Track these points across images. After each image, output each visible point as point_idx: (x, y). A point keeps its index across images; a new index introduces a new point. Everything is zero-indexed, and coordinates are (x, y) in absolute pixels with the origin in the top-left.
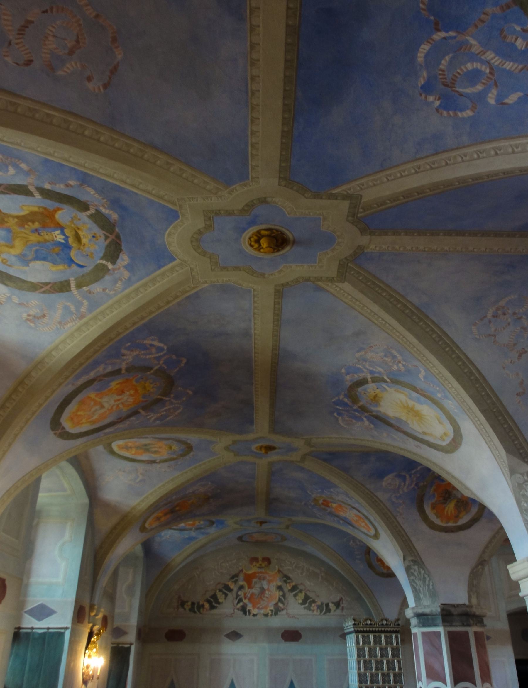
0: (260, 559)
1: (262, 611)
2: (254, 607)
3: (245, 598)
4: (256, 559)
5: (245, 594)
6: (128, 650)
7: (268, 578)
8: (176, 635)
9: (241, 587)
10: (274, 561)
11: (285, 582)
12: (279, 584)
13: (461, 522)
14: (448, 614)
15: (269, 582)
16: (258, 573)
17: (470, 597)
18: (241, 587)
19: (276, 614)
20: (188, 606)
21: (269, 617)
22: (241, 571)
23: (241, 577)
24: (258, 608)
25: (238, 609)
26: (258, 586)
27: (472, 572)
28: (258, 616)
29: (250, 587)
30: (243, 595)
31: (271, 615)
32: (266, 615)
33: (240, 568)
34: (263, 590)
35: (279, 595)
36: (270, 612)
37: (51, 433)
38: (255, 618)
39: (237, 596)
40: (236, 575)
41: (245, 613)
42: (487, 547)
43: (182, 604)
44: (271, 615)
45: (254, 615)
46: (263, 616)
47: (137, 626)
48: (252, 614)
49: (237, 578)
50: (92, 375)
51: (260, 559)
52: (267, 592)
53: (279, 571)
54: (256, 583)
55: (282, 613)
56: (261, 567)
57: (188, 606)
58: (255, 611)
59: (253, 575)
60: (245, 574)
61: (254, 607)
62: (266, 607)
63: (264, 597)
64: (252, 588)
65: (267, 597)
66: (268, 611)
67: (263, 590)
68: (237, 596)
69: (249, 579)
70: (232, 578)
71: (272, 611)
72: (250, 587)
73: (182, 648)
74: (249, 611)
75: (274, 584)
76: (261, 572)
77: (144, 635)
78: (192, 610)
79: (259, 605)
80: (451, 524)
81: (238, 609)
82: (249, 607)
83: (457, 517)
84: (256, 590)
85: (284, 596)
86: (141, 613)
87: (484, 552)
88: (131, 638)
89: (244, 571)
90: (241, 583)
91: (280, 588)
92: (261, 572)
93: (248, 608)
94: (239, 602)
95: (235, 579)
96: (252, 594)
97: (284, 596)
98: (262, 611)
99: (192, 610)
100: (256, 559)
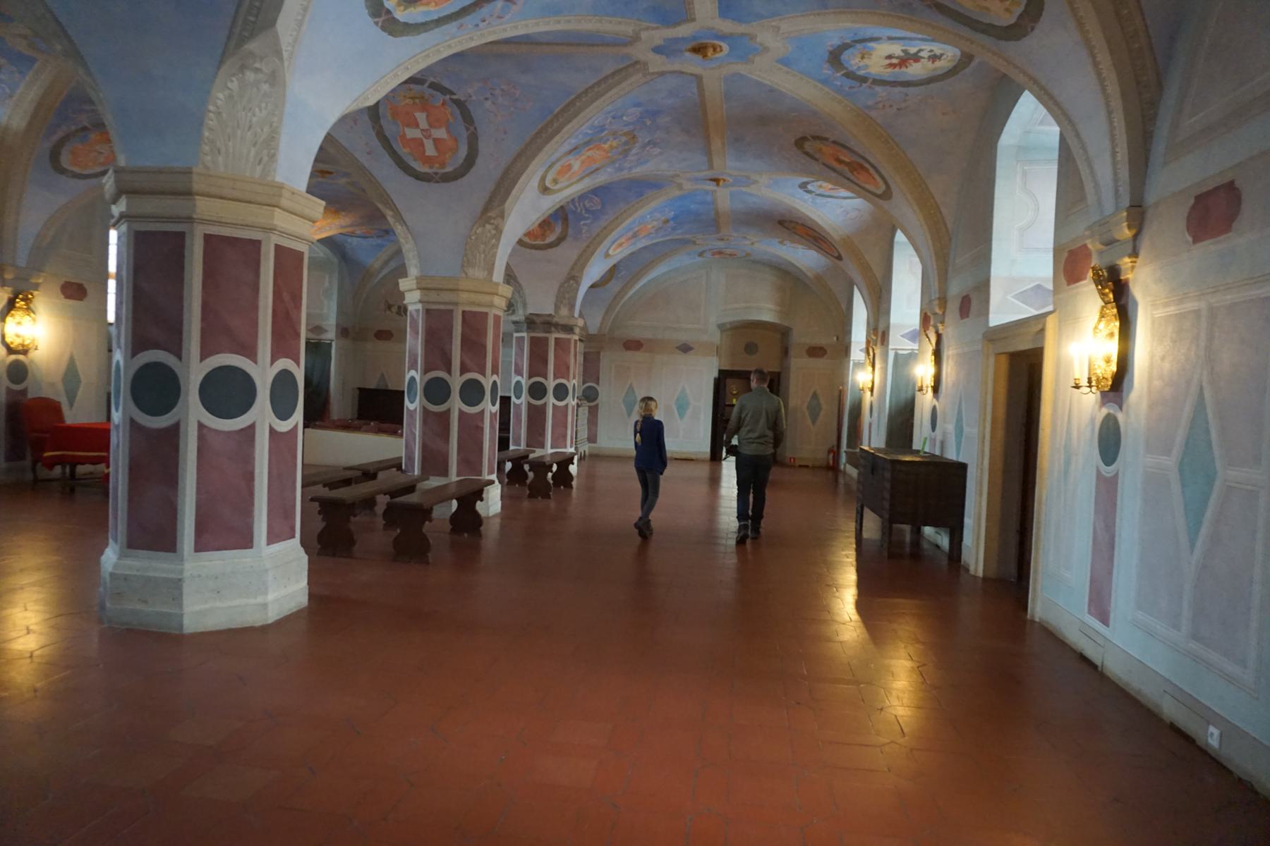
6: (330, 345)
8: (384, 335)
13: (548, 240)
14: (531, 323)
17: (557, 308)
20: (394, 309)
27: (561, 286)
37: (64, 177)
42: (575, 264)
43: (389, 307)
47: (337, 325)
50: (60, 134)
57: (394, 309)
73: (383, 345)
77: (343, 332)
78: (399, 313)
80: (539, 242)
83: (543, 236)
86: (341, 312)
87: (573, 269)
88: (330, 335)
99: (399, 313)
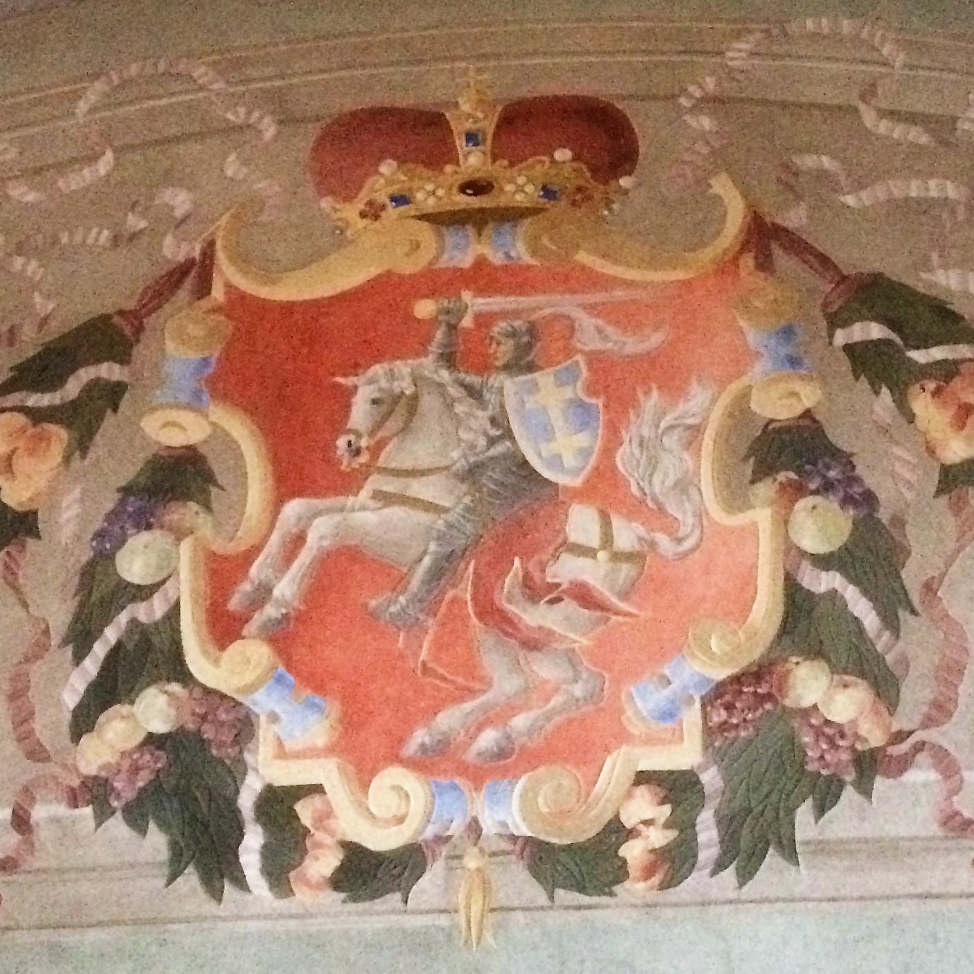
0: (469, 111)
1: (508, 811)
2: (363, 750)
3: (224, 629)
4: (419, 133)
5: (223, 572)
7: (592, 334)
9: (177, 479)
10: (675, 135)
11: (871, 363)
12: (780, 400)
15: (614, 390)
16: (439, 282)
18: (177, 479)
19: (756, 838)
21: (635, 888)
22: (197, 273)
23: (181, 345)
24: (436, 761)
25: (94, 793)
26: (433, 452)
28: (428, 886)
29: (304, 467)
30: (187, 590)
31: (675, 862)
32: (581, 865)
33: (175, 250)
34: (513, 498)
35: (792, 554)
36: (642, 808)
38: (379, 916)
39: (99, 593)
40: (109, 337)
41: (207, 848)
44: (675, 862)
45: (364, 873)
46: (517, 883)
48: (323, 862)
49: (109, 371)
51: (469, 111)
52: (582, 523)
53: (763, 237)
54: (399, 410)
55: (847, 818)
56: (478, 212)
58: (385, 810)
59: (374, 320)
60: (239, 302)
61: (363, 750)
62: (577, 742)
63: (534, 590)
64: (348, 483)
65: (584, 596)
66: (613, 789)
67: (513, 498)
68: (99, 593)
69: (293, 376)
70: (44, 369)
71: (677, 789)
72: (304, 467)
74: (279, 805)
75: (703, 402)
76: (482, 277)
79: (449, 719)
81: (94, 793)
82: (289, 743)
84: (400, 508)
85: (873, 554)
89: (227, 273)
90: (173, 426)
91: (792, 455)
92: (482, 277)
93: (264, 769)
94: (109, 691)
95: (73, 388)
96: (343, 567)
97: (873, 554)
98: (508, 811)
100: (419, 133)
